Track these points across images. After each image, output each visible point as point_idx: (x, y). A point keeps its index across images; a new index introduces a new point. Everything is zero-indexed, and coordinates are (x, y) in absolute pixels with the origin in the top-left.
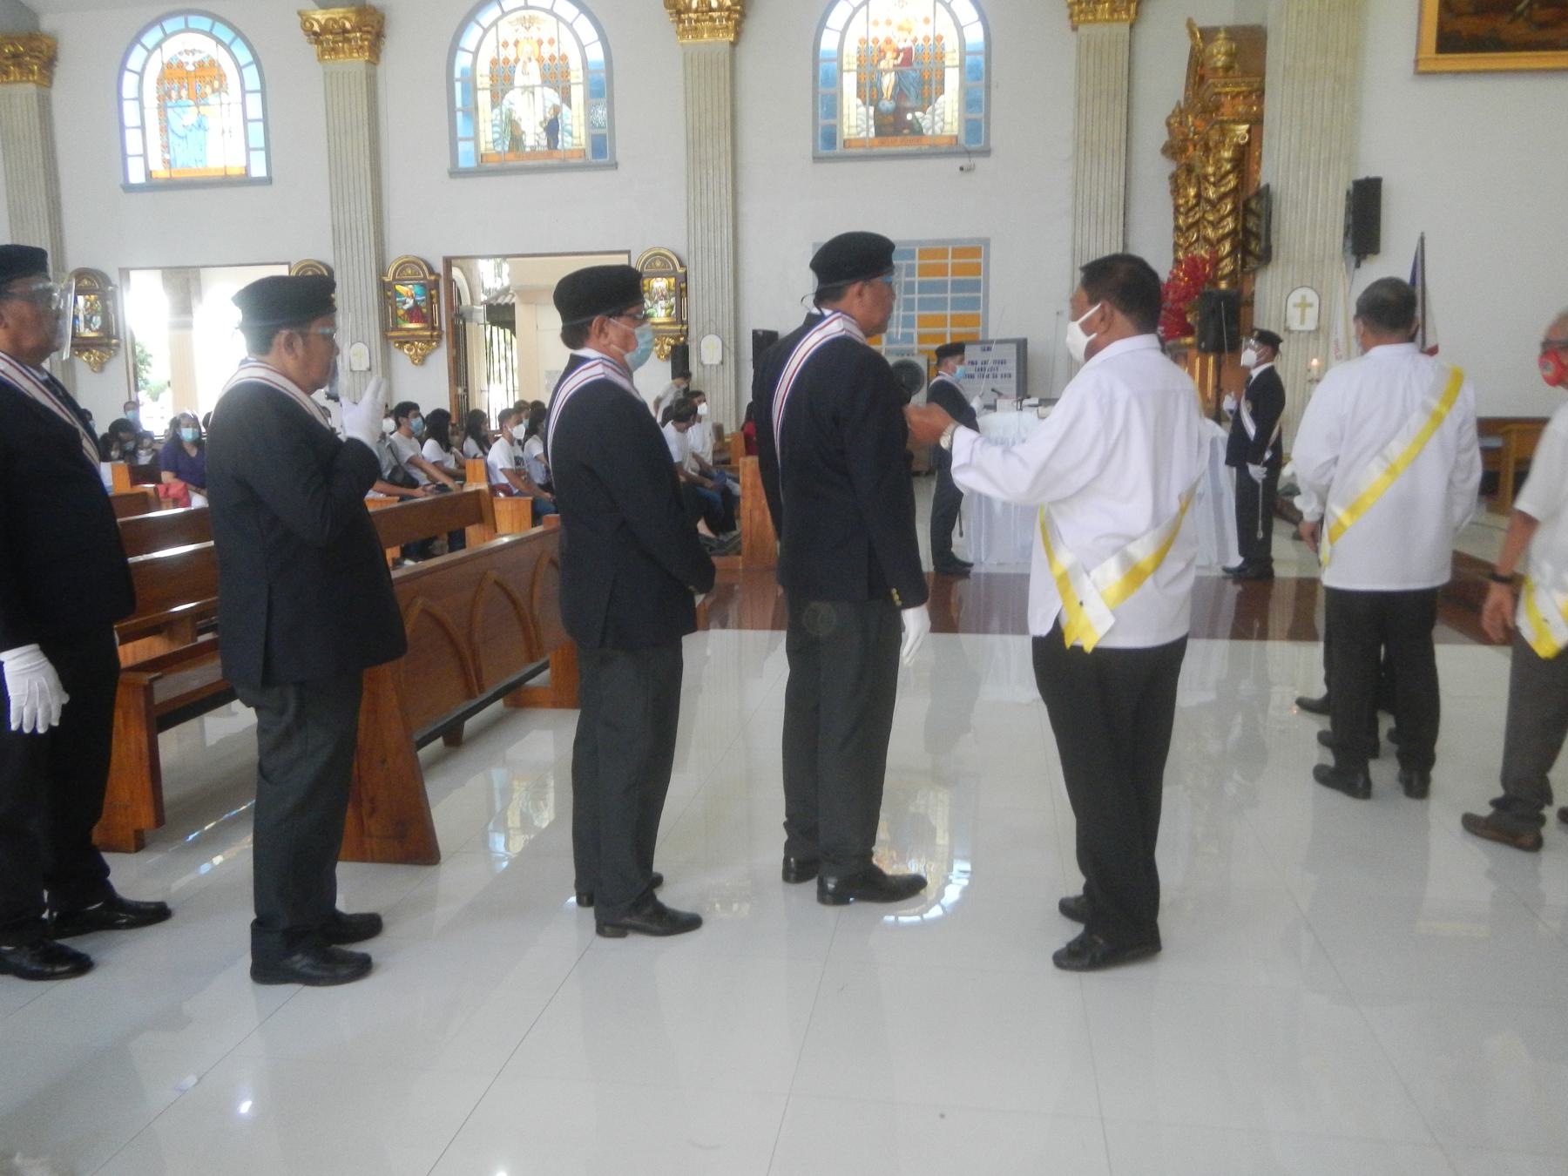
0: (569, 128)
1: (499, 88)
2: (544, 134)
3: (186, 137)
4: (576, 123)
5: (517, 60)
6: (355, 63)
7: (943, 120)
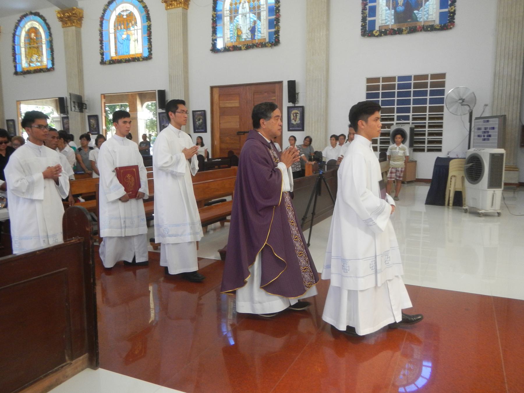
0: (260, 29)
1: (233, 15)
2: (250, 33)
3: (123, 43)
4: (262, 28)
5: (240, 3)
7: (428, 14)
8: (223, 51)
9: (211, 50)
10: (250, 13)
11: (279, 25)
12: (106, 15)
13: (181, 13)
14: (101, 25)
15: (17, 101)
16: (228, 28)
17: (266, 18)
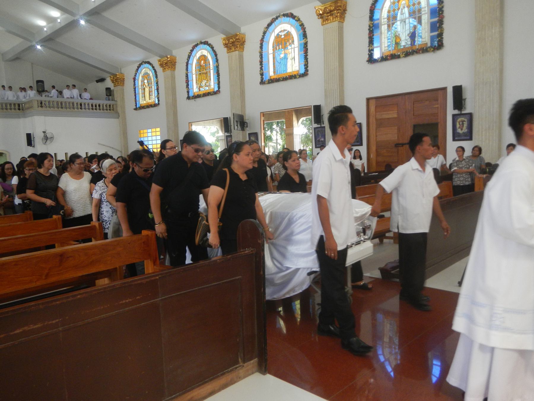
0: (420, 34)
1: (391, 23)
2: (409, 39)
6: (334, 25)
8: (380, 61)
9: (367, 61)
10: (409, 19)
11: (442, 27)
12: (265, 37)
13: (337, 27)
14: (261, 47)
15: (189, 123)
16: (386, 37)
17: (428, 22)
